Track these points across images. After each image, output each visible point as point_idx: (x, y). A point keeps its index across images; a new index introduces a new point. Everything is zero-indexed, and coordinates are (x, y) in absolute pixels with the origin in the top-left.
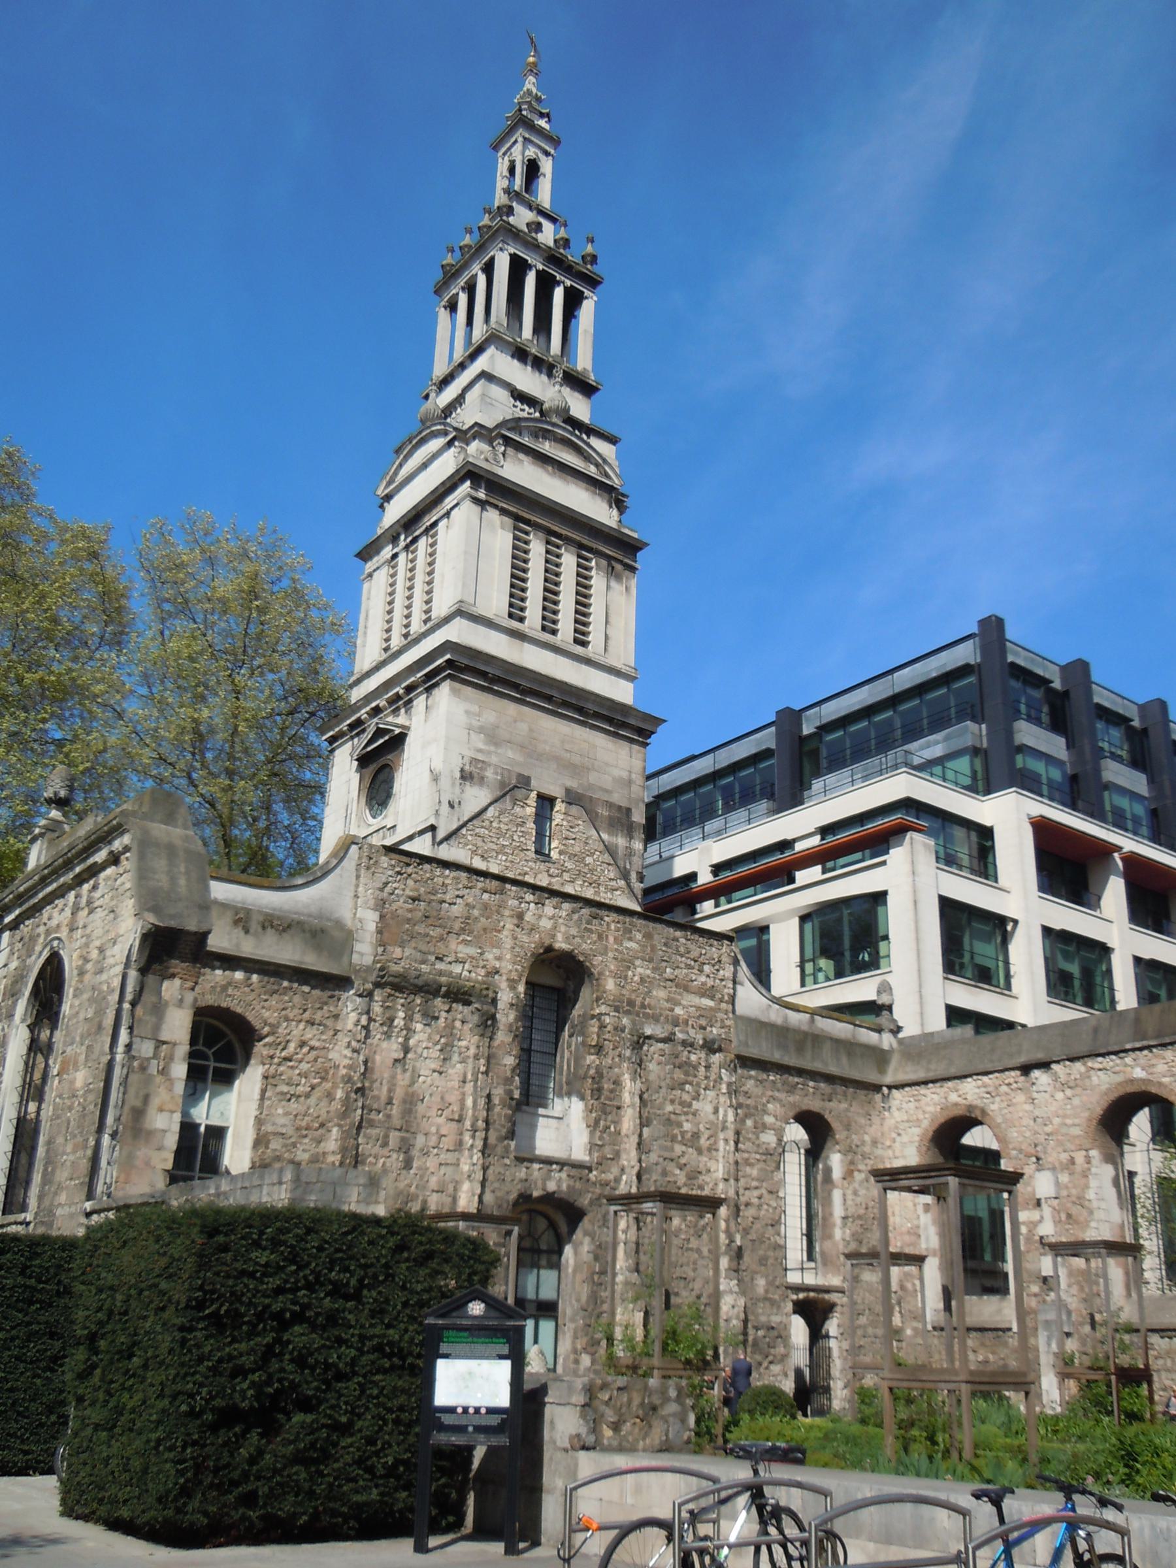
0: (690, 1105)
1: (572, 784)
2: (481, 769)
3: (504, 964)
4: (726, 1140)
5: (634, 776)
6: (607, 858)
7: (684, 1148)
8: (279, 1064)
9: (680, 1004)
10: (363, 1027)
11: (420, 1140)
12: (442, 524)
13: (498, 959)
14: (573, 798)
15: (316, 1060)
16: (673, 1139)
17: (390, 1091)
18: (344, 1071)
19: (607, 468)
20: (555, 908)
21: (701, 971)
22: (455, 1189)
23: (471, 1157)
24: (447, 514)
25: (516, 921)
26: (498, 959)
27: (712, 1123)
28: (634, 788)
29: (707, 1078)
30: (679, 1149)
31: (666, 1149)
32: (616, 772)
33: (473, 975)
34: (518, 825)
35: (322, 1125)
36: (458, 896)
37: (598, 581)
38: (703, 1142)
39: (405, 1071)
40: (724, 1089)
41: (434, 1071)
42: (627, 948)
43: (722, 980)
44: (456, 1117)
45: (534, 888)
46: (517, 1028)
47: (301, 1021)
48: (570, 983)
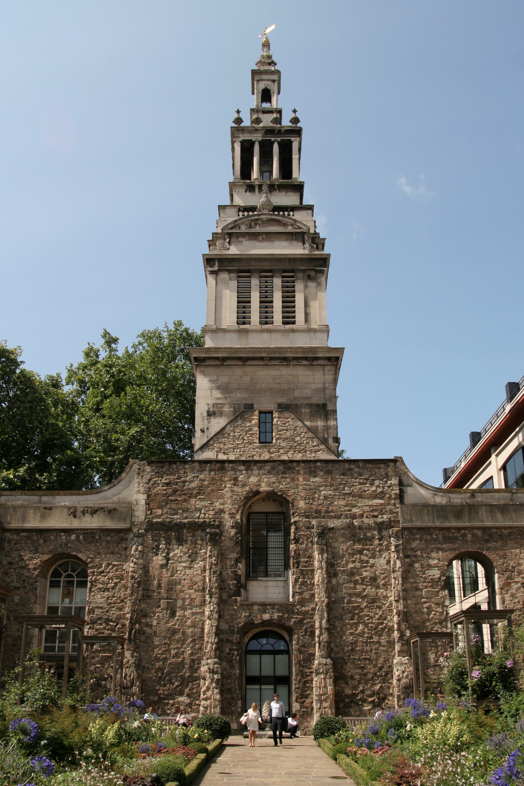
0: (367, 562)
1: (283, 400)
2: (220, 408)
3: (226, 506)
4: (395, 578)
5: (327, 385)
6: (310, 434)
7: (364, 587)
8: (97, 576)
9: (356, 506)
10: (140, 551)
11: (179, 603)
13: (222, 504)
14: (283, 408)
15: (116, 571)
16: (356, 582)
17: (159, 580)
18: (130, 574)
19: (297, 224)
20: (259, 470)
22: (203, 624)
23: (210, 608)
26: (222, 504)
27: (386, 569)
28: (327, 392)
29: (380, 545)
30: (359, 588)
31: (350, 588)
32: (314, 386)
33: (207, 515)
34: (247, 432)
35: (122, 601)
36: (194, 477)
37: (299, 286)
38: (379, 580)
39: (168, 570)
40: (393, 548)
41: (185, 567)
42: (313, 482)
43: (389, 487)
44: (201, 588)
45: (244, 462)
46: (237, 538)
47: (107, 553)
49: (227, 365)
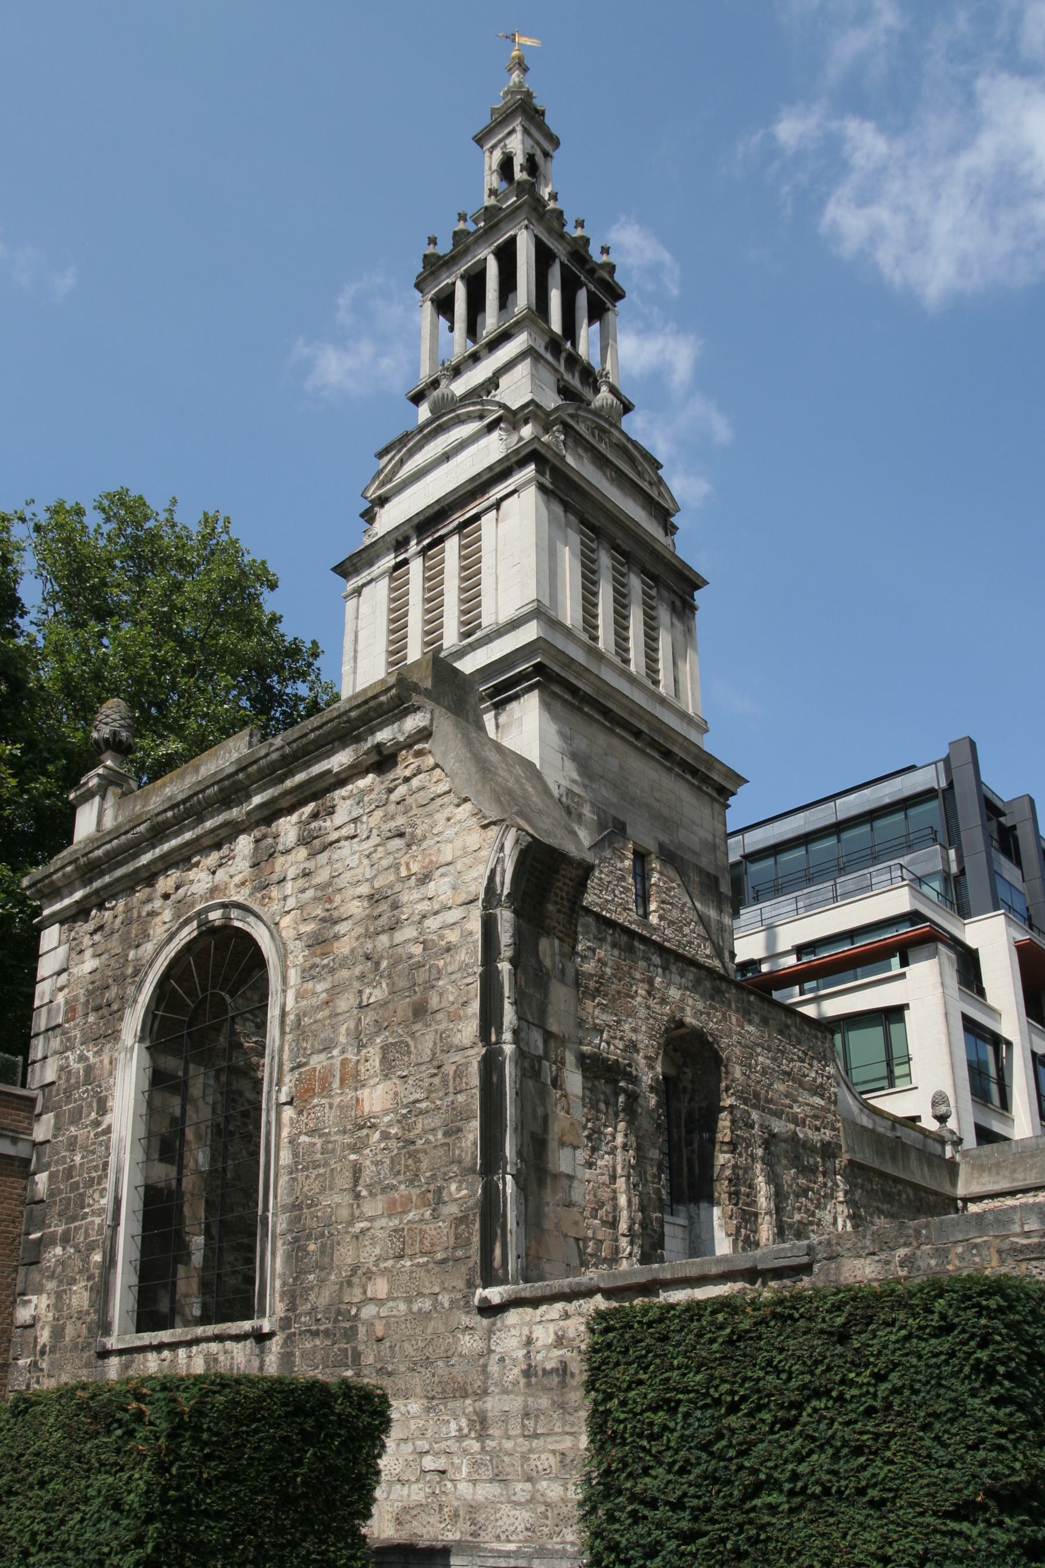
1: (664, 838)
3: (640, 1037)
12: (488, 520)
13: (634, 1030)
21: (811, 1065)
24: (497, 505)
25: (646, 987)
46: (659, 1116)
48: (687, 1070)
49: (587, 715)
